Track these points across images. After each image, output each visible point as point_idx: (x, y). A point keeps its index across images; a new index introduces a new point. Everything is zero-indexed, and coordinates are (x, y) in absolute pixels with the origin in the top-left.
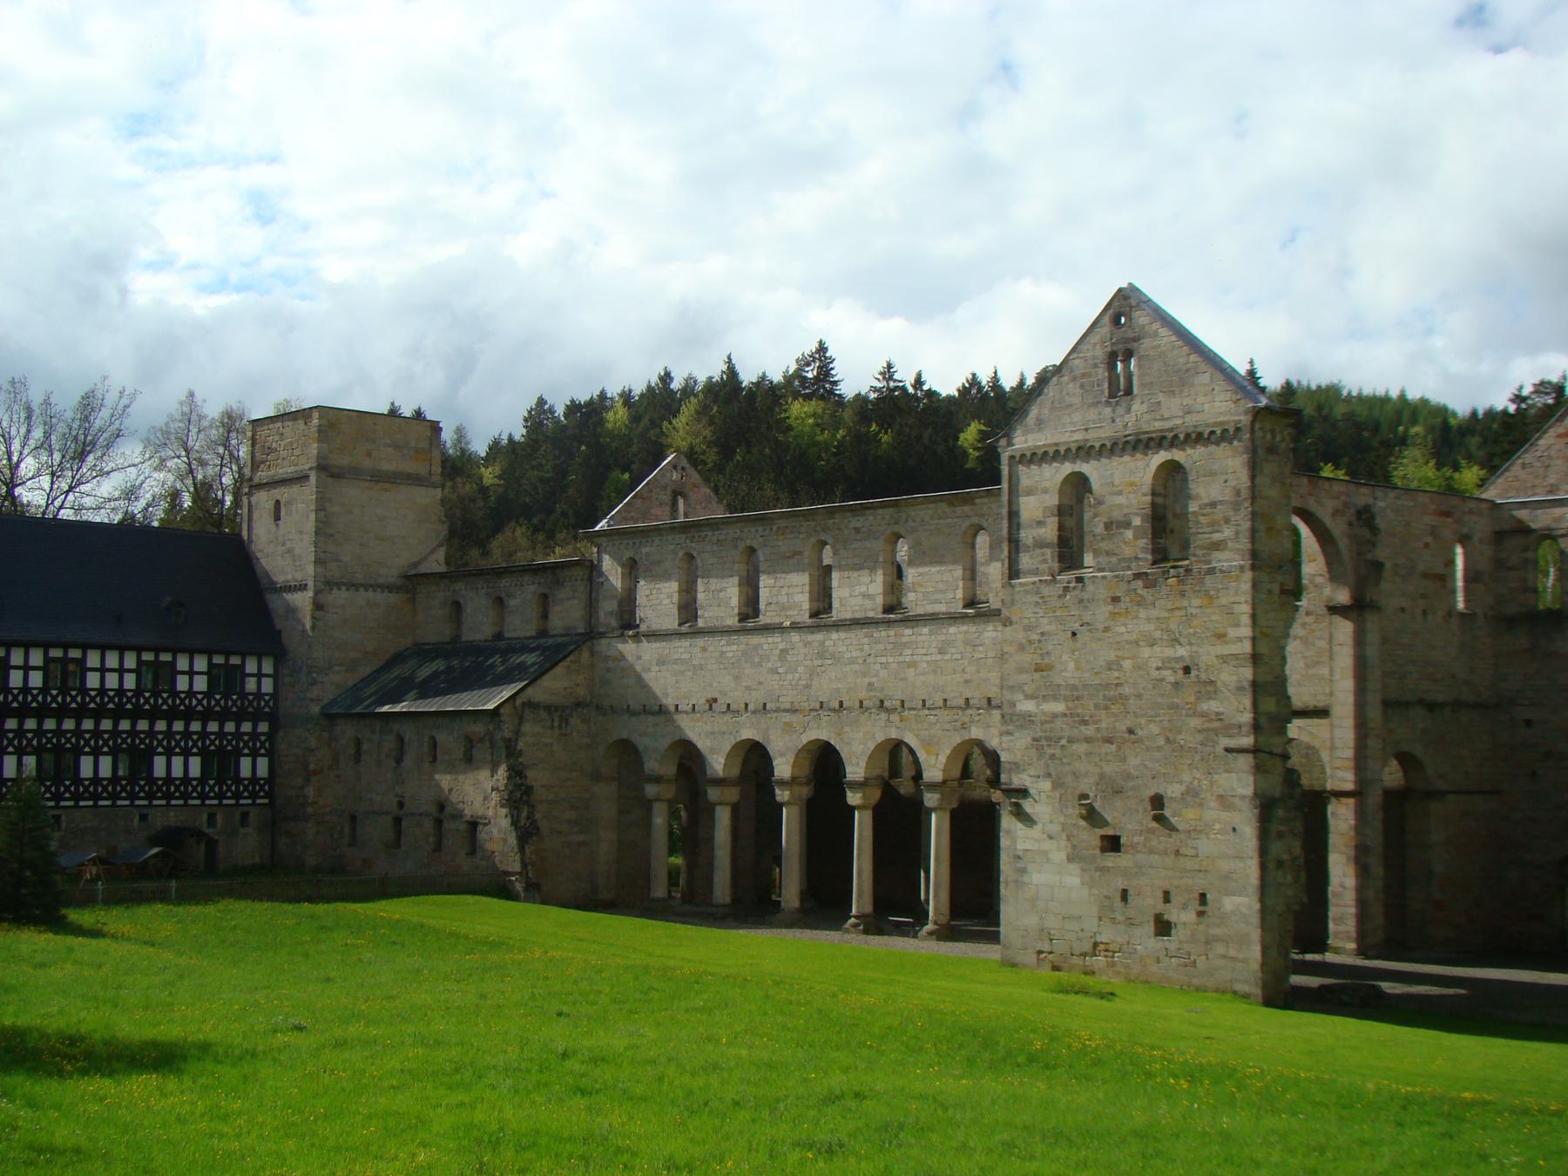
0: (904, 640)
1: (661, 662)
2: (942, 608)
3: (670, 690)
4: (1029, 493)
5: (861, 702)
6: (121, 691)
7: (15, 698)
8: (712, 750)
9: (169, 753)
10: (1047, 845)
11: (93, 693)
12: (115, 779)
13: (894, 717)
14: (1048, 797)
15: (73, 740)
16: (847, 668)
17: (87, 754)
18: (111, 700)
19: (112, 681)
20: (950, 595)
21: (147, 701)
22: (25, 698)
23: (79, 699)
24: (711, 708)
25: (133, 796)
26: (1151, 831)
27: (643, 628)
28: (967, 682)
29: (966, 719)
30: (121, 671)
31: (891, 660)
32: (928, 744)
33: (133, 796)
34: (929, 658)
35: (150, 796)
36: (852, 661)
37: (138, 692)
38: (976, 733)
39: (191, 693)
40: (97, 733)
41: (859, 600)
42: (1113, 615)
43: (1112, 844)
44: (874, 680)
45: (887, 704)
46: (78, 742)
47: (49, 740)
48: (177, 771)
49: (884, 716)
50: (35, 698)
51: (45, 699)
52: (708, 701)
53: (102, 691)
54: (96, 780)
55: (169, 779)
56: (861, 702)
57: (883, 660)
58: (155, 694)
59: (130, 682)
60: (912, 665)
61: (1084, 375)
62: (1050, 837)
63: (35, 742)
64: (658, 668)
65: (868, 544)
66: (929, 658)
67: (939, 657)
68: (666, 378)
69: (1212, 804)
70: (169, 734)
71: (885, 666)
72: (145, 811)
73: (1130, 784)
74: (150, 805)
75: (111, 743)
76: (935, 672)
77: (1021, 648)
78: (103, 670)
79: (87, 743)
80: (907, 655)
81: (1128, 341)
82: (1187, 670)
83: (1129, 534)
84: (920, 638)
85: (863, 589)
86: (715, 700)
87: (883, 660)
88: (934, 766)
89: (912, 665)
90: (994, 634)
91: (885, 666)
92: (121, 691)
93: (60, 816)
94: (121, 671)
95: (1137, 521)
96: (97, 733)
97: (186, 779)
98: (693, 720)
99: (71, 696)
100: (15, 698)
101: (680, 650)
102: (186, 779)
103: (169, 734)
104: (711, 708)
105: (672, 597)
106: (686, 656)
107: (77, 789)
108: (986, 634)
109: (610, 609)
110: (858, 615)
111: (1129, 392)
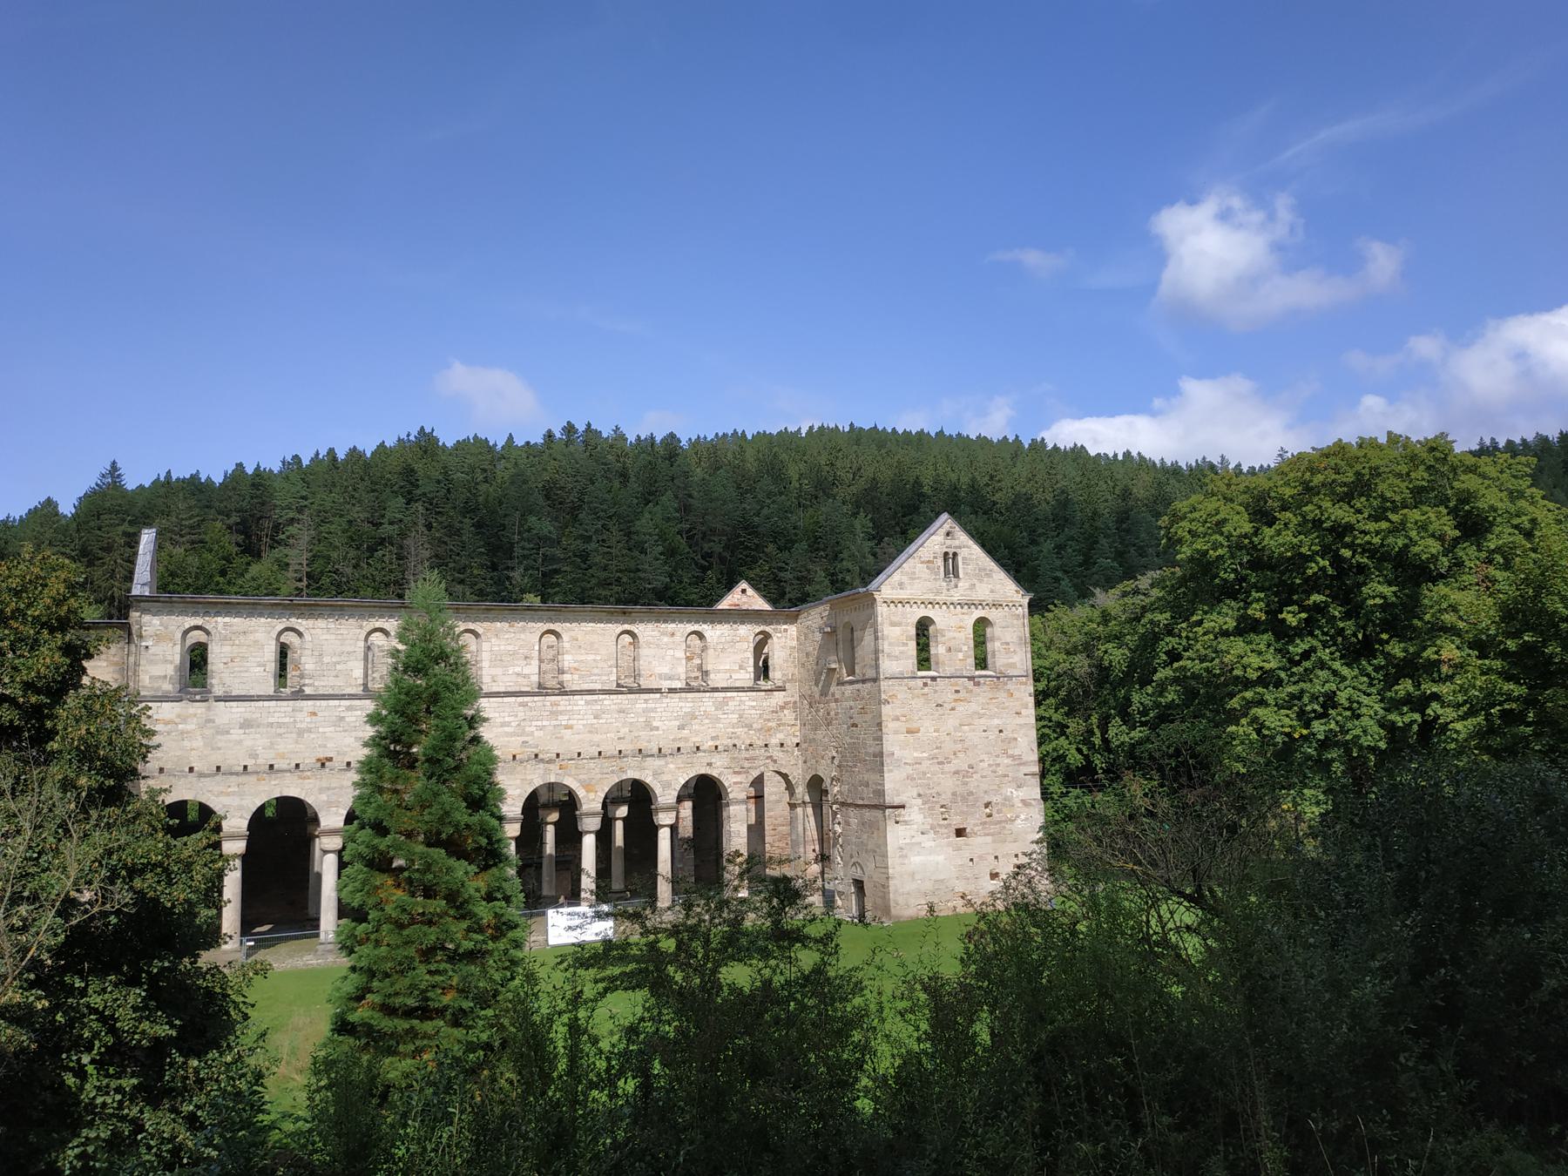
0: (559, 708)
1: (246, 725)
2: (598, 687)
3: (260, 750)
4: (893, 624)
5: (514, 757)
8: (330, 804)
10: (919, 838)
13: (554, 767)
14: (920, 809)
16: (500, 730)
20: (605, 678)
24: (323, 765)
26: (985, 823)
27: (218, 690)
28: (619, 739)
29: (623, 765)
31: (548, 723)
32: (589, 787)
34: (585, 722)
36: (503, 724)
38: (632, 774)
41: (514, 678)
42: (956, 700)
43: (960, 833)
44: (526, 739)
45: (540, 756)
49: (541, 765)
52: (318, 760)
56: (514, 757)
57: (539, 723)
60: (568, 727)
61: (929, 562)
62: (922, 833)
64: (242, 731)
65: (523, 636)
66: (580, 722)
67: (595, 721)
68: (240, 466)
69: (1020, 805)
71: (541, 728)
73: (971, 798)
76: (590, 732)
77: (897, 719)
80: (563, 719)
81: (956, 547)
82: (1001, 731)
83: (961, 656)
84: (575, 708)
85: (518, 669)
86: (330, 759)
87: (539, 723)
88: (594, 800)
89: (568, 727)
90: (645, 705)
91: (541, 728)
95: (965, 648)
98: (300, 778)
101: (276, 715)
104: (323, 765)
105: (264, 666)
106: (287, 720)
108: (637, 706)
109: (163, 674)
110: (510, 690)
111: (956, 575)
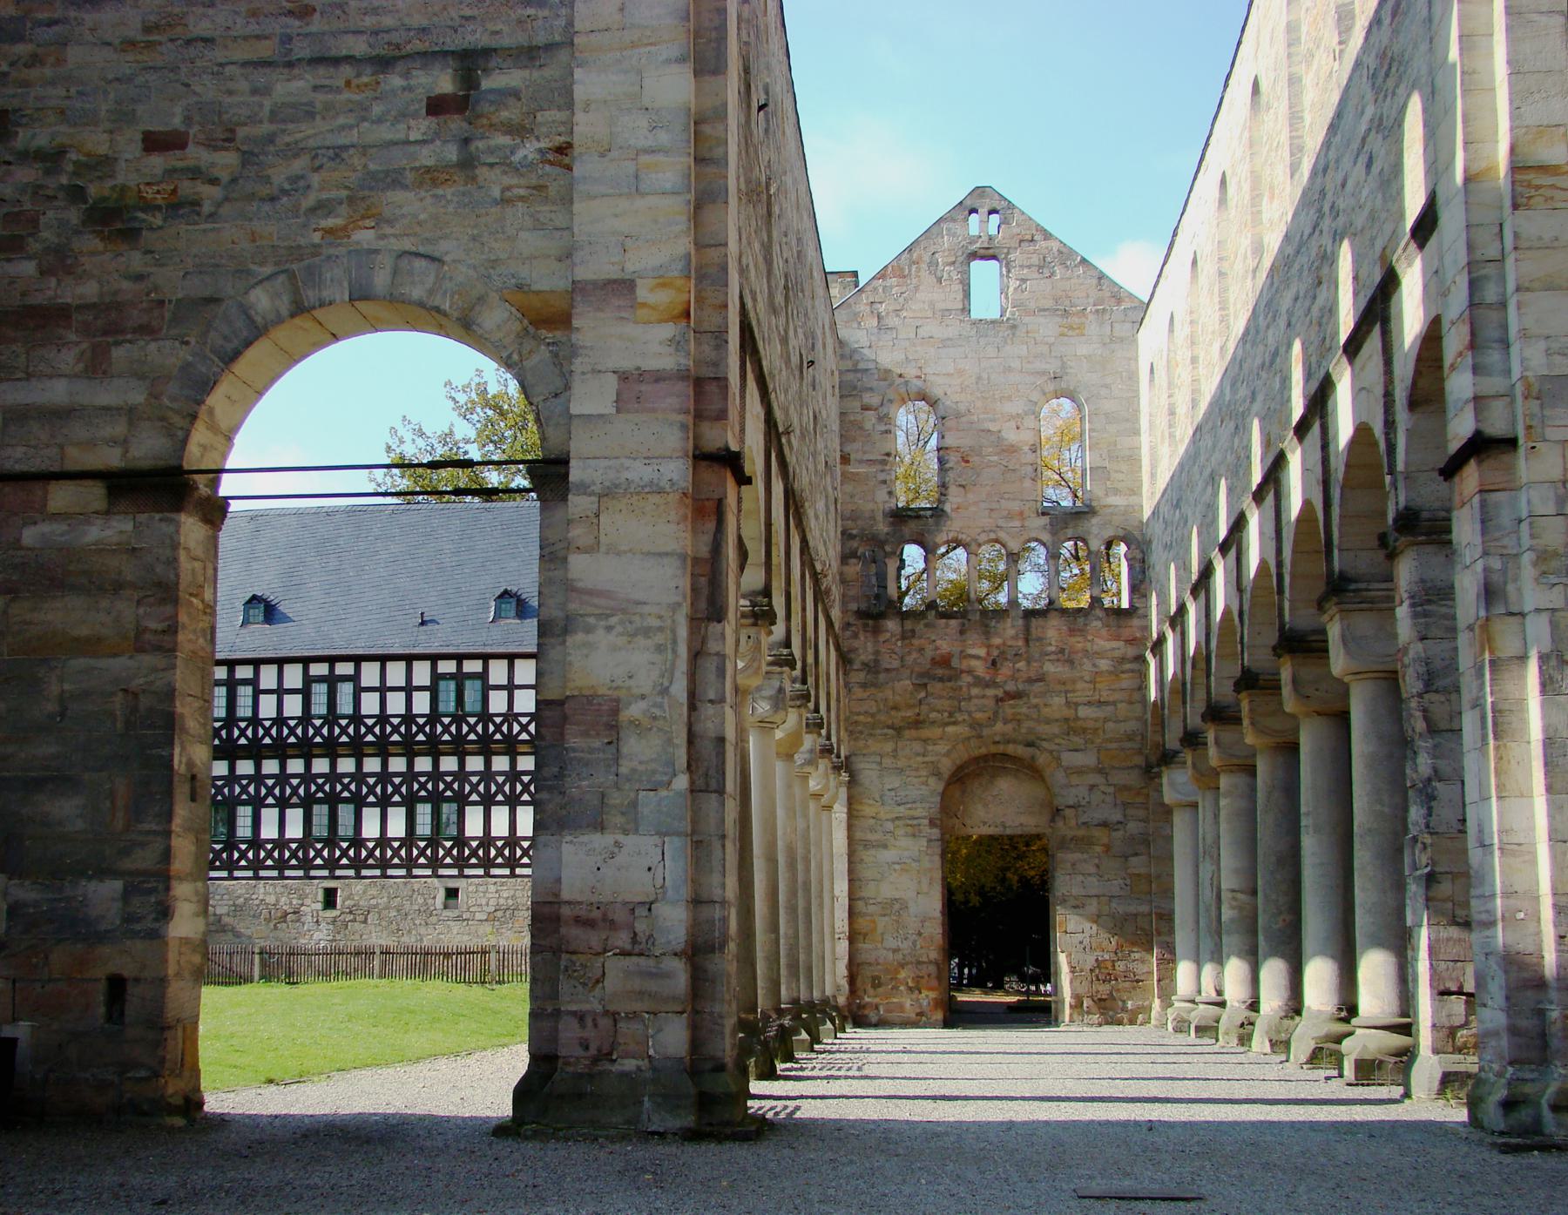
6: (409, 718)
7: (267, 732)
9: (488, 802)
11: (370, 722)
12: (410, 838)
15: (353, 787)
17: (372, 805)
18: (396, 729)
19: (396, 704)
21: (446, 729)
22: (280, 732)
23: (351, 730)
25: (435, 863)
30: (409, 689)
33: (435, 863)
35: (461, 863)
37: (434, 717)
39: (510, 716)
40: (384, 776)
46: (359, 789)
47: (320, 788)
48: (500, 827)
50: (292, 731)
51: (305, 731)
53: (383, 718)
54: (383, 841)
55: (487, 840)
58: (459, 719)
59: (422, 703)
63: (301, 791)
70: (487, 775)
72: (452, 884)
74: (462, 875)
75: (404, 789)
78: (383, 690)
79: (371, 791)
92: (409, 718)
93: (335, 890)
94: (409, 689)
96: (384, 776)
97: (512, 840)
99: (340, 726)
100: (267, 732)
102: (512, 840)
103: (487, 775)
107: (358, 853)
